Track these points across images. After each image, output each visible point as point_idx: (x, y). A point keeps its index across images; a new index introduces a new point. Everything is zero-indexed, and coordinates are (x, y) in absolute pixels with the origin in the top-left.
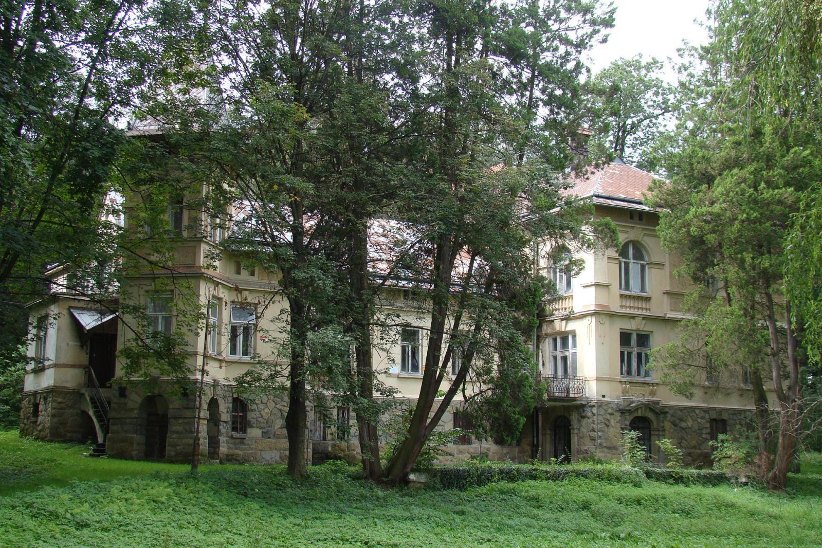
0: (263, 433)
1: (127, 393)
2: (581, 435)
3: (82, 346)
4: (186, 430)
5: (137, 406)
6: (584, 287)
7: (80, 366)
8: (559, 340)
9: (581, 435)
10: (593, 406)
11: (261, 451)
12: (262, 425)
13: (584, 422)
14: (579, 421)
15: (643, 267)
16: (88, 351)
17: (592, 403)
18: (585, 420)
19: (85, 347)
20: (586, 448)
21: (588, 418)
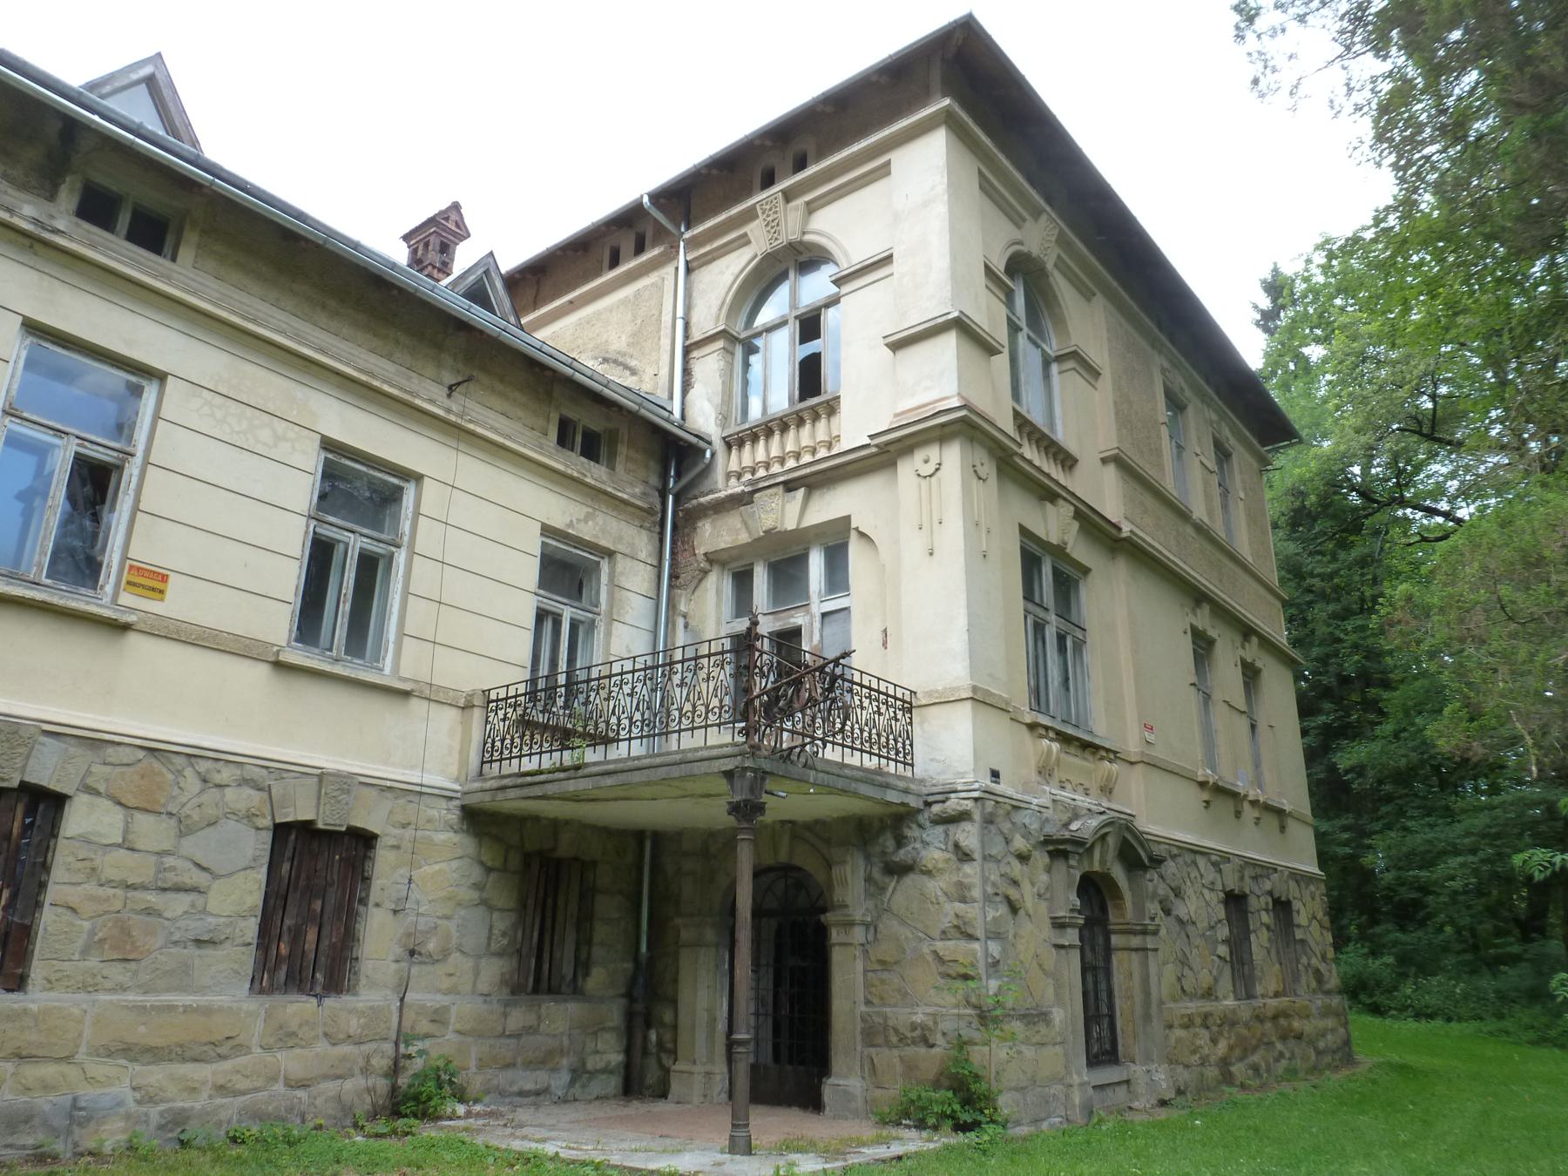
2: (885, 951)
6: (897, 346)
8: (761, 580)
9: (885, 951)
10: (962, 817)
13: (902, 893)
14: (875, 889)
15: (1047, 362)
17: (954, 804)
18: (910, 880)
20: (919, 1018)
21: (929, 873)
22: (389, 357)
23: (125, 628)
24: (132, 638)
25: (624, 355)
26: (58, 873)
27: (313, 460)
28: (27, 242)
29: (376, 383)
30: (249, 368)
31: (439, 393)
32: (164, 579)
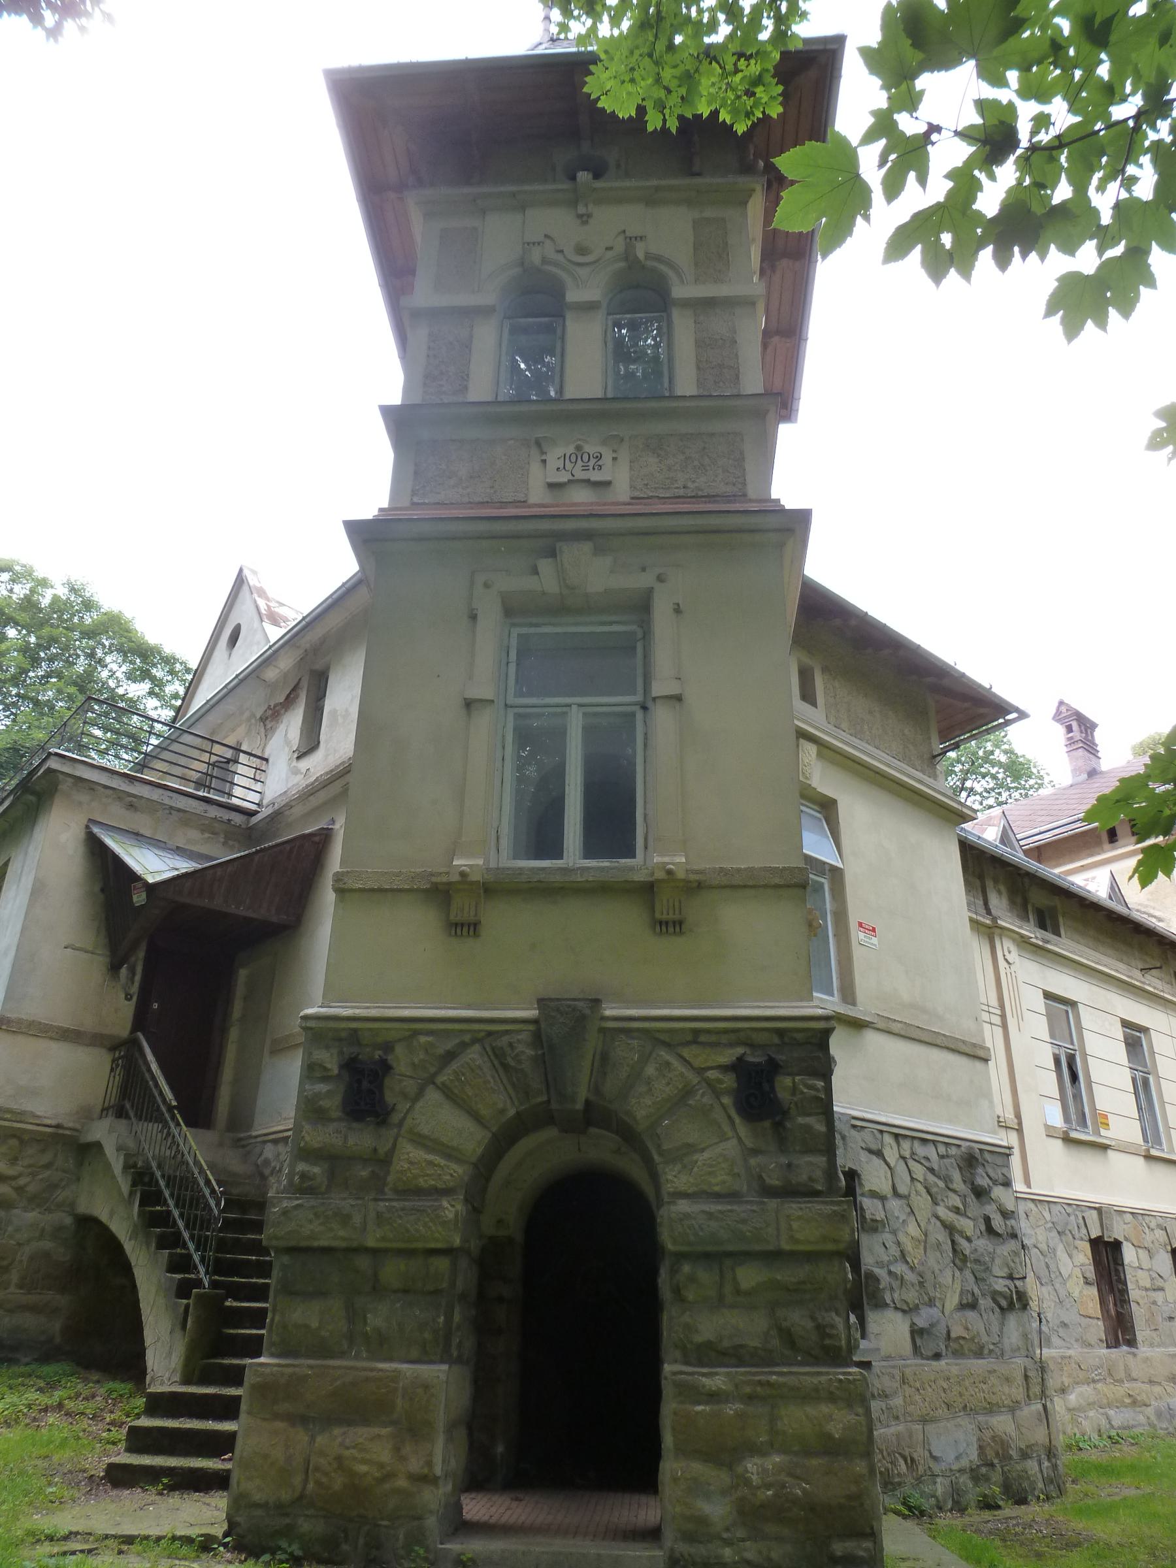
0: (917, 1333)
1: (390, 1098)
3: (114, 968)
4: (788, 1337)
5: (456, 1172)
7: (95, 1040)
11: (924, 1420)
12: (911, 1296)
16: (135, 989)
19: (124, 971)
22: (1121, 961)
23: (1104, 1148)
24: (1110, 1152)
25: (1147, 906)
26: (1130, 1286)
27: (1119, 1033)
28: (1035, 949)
29: (1133, 981)
30: (1094, 988)
31: (1138, 974)
32: (1106, 1117)
